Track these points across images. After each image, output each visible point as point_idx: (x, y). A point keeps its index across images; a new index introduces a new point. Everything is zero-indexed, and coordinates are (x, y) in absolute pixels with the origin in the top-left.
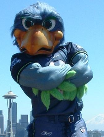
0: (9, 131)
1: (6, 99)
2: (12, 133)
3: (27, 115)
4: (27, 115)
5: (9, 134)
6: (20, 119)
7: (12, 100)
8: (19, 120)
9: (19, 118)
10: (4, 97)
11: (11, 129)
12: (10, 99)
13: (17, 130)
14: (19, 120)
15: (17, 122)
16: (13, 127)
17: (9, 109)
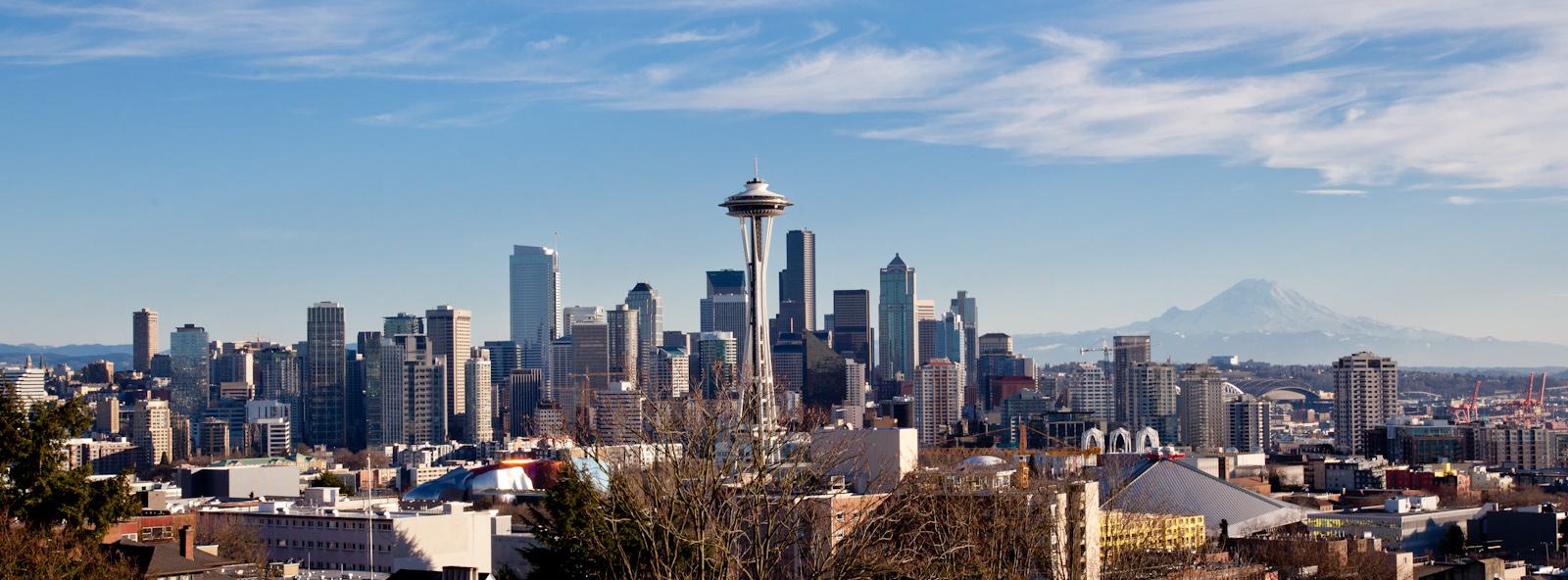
1: (736, 220)
2: (770, 380)
3: (862, 294)
4: (862, 294)
6: (831, 311)
7: (762, 218)
8: (827, 317)
9: (825, 306)
10: (726, 210)
11: (766, 359)
12: (758, 219)
13: (809, 366)
14: (827, 317)
15: (818, 329)
16: (775, 349)
17: (753, 264)
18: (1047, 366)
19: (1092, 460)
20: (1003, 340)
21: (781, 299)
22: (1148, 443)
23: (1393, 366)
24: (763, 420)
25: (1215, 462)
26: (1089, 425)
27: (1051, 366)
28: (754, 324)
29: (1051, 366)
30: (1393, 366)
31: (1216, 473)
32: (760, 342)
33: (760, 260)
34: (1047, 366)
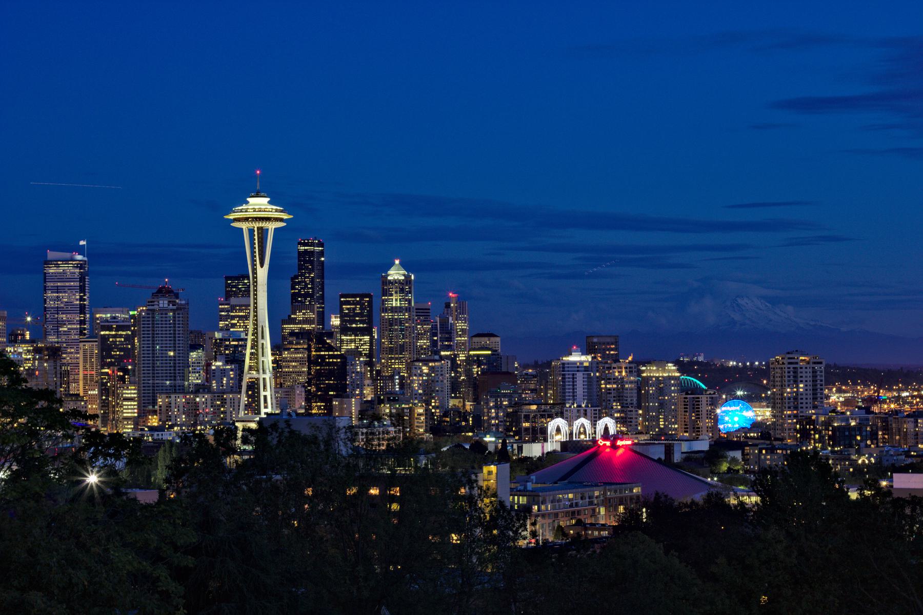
0: (258, 371)
5: (258, 379)
18: (536, 362)
19: (558, 447)
20: (492, 339)
21: (292, 303)
22: (606, 429)
23: (821, 363)
24: (263, 411)
25: (663, 449)
26: (561, 415)
27: (540, 363)
28: (256, 325)
29: (540, 363)
30: (821, 363)
31: (663, 458)
32: (261, 341)
33: (262, 266)
34: (536, 362)
